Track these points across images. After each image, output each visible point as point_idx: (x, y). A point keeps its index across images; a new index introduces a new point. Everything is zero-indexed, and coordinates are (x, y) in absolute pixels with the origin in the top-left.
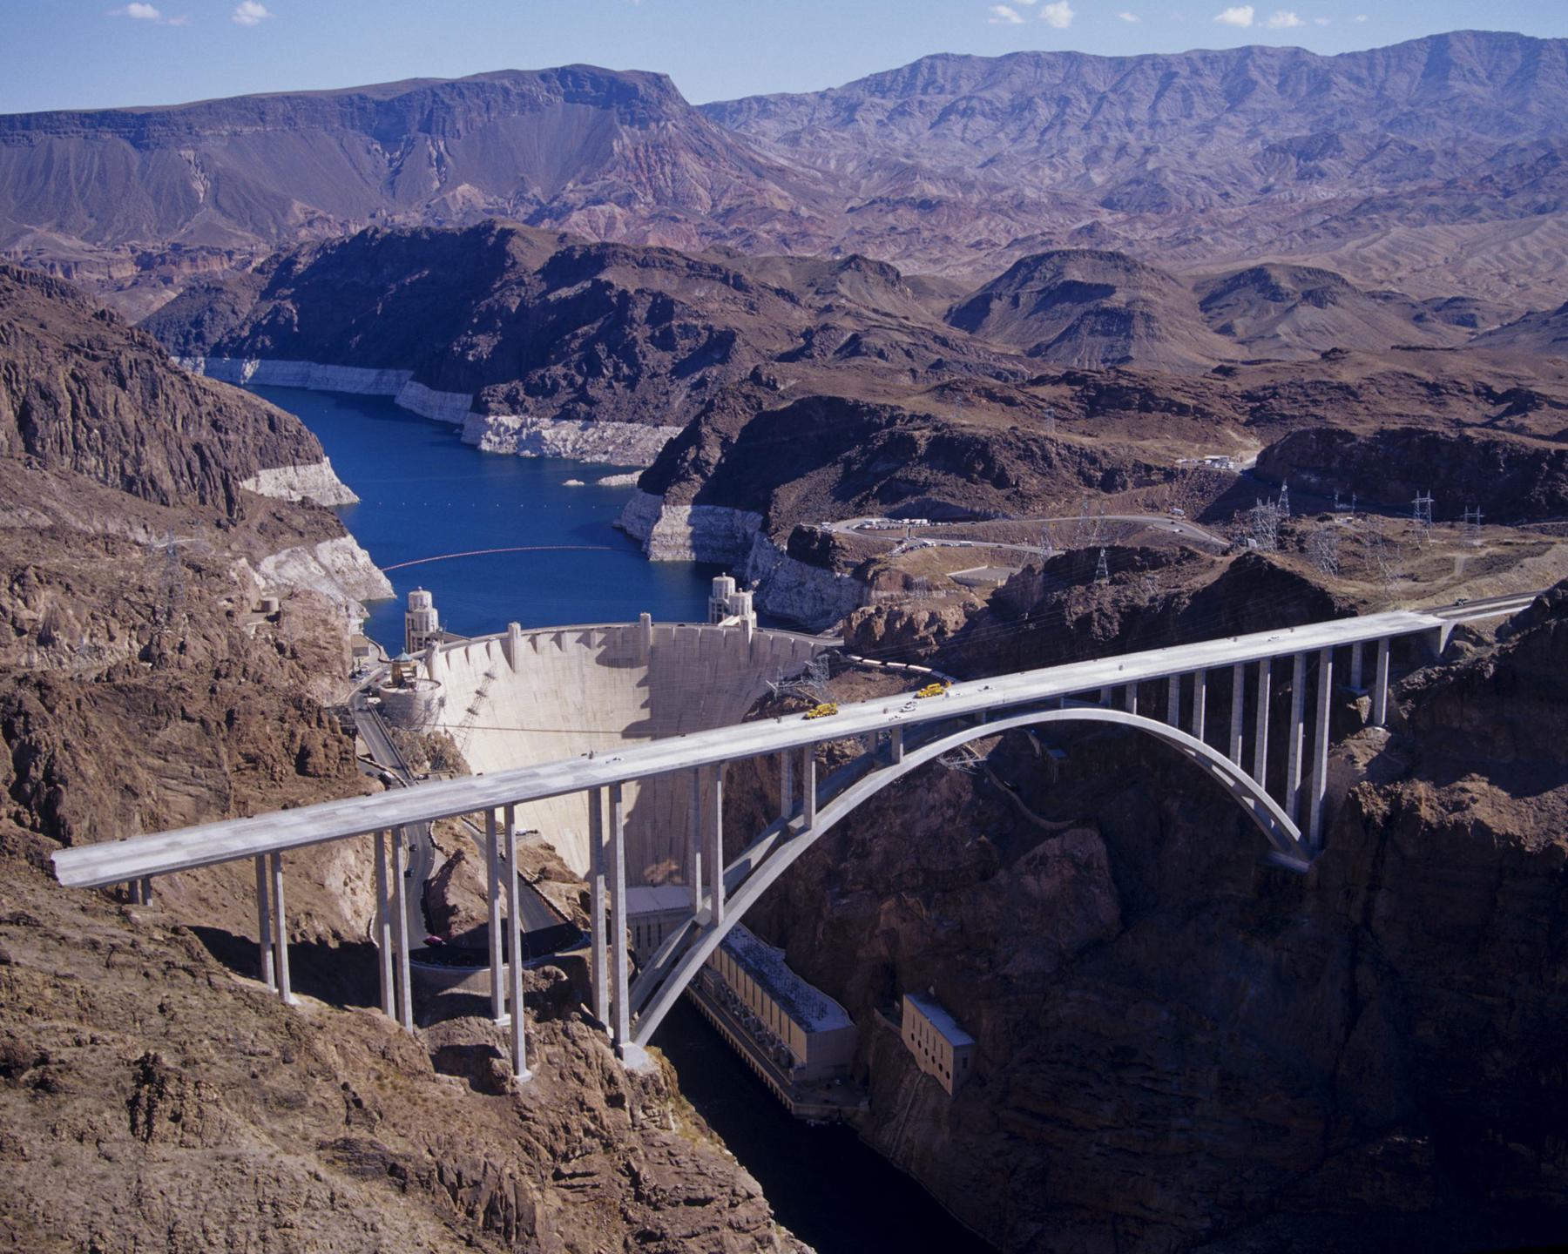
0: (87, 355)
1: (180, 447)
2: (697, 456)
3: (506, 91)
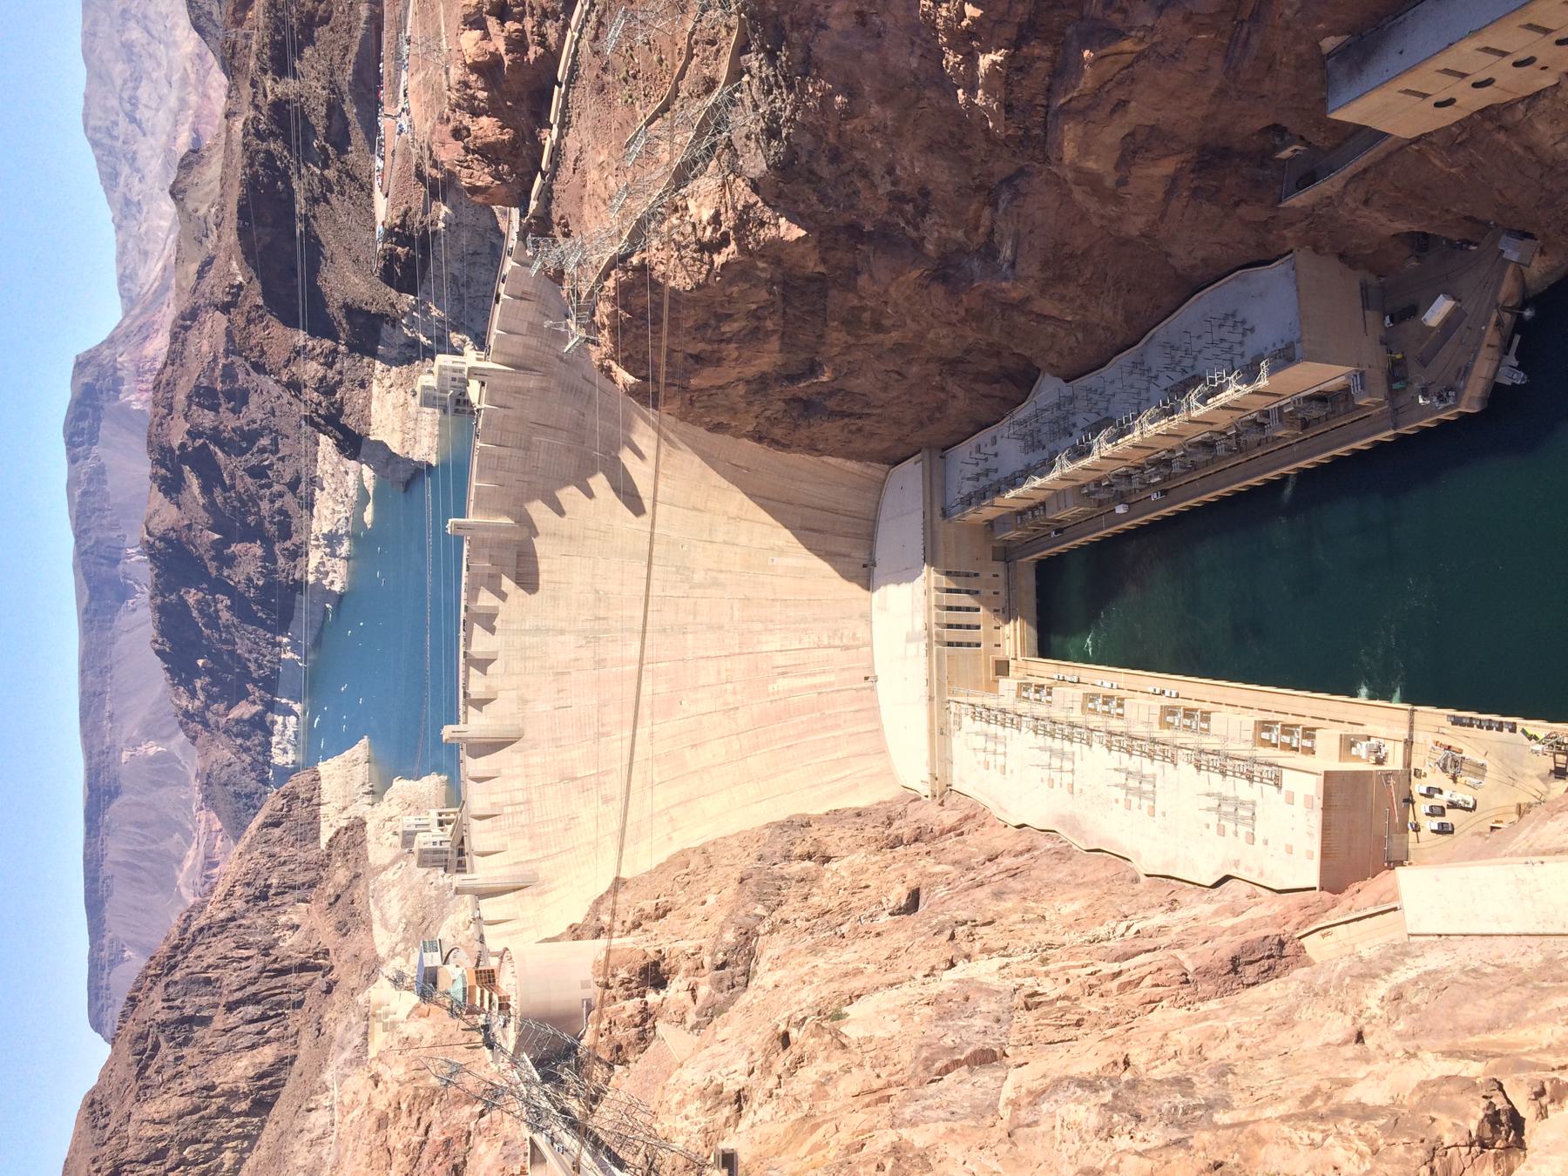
0: (152, 1057)
1: (226, 1031)
2: (316, 390)
3: (84, 494)
